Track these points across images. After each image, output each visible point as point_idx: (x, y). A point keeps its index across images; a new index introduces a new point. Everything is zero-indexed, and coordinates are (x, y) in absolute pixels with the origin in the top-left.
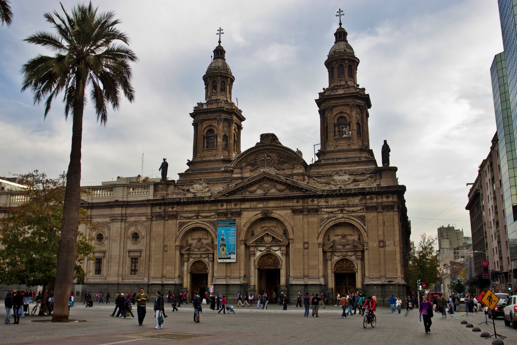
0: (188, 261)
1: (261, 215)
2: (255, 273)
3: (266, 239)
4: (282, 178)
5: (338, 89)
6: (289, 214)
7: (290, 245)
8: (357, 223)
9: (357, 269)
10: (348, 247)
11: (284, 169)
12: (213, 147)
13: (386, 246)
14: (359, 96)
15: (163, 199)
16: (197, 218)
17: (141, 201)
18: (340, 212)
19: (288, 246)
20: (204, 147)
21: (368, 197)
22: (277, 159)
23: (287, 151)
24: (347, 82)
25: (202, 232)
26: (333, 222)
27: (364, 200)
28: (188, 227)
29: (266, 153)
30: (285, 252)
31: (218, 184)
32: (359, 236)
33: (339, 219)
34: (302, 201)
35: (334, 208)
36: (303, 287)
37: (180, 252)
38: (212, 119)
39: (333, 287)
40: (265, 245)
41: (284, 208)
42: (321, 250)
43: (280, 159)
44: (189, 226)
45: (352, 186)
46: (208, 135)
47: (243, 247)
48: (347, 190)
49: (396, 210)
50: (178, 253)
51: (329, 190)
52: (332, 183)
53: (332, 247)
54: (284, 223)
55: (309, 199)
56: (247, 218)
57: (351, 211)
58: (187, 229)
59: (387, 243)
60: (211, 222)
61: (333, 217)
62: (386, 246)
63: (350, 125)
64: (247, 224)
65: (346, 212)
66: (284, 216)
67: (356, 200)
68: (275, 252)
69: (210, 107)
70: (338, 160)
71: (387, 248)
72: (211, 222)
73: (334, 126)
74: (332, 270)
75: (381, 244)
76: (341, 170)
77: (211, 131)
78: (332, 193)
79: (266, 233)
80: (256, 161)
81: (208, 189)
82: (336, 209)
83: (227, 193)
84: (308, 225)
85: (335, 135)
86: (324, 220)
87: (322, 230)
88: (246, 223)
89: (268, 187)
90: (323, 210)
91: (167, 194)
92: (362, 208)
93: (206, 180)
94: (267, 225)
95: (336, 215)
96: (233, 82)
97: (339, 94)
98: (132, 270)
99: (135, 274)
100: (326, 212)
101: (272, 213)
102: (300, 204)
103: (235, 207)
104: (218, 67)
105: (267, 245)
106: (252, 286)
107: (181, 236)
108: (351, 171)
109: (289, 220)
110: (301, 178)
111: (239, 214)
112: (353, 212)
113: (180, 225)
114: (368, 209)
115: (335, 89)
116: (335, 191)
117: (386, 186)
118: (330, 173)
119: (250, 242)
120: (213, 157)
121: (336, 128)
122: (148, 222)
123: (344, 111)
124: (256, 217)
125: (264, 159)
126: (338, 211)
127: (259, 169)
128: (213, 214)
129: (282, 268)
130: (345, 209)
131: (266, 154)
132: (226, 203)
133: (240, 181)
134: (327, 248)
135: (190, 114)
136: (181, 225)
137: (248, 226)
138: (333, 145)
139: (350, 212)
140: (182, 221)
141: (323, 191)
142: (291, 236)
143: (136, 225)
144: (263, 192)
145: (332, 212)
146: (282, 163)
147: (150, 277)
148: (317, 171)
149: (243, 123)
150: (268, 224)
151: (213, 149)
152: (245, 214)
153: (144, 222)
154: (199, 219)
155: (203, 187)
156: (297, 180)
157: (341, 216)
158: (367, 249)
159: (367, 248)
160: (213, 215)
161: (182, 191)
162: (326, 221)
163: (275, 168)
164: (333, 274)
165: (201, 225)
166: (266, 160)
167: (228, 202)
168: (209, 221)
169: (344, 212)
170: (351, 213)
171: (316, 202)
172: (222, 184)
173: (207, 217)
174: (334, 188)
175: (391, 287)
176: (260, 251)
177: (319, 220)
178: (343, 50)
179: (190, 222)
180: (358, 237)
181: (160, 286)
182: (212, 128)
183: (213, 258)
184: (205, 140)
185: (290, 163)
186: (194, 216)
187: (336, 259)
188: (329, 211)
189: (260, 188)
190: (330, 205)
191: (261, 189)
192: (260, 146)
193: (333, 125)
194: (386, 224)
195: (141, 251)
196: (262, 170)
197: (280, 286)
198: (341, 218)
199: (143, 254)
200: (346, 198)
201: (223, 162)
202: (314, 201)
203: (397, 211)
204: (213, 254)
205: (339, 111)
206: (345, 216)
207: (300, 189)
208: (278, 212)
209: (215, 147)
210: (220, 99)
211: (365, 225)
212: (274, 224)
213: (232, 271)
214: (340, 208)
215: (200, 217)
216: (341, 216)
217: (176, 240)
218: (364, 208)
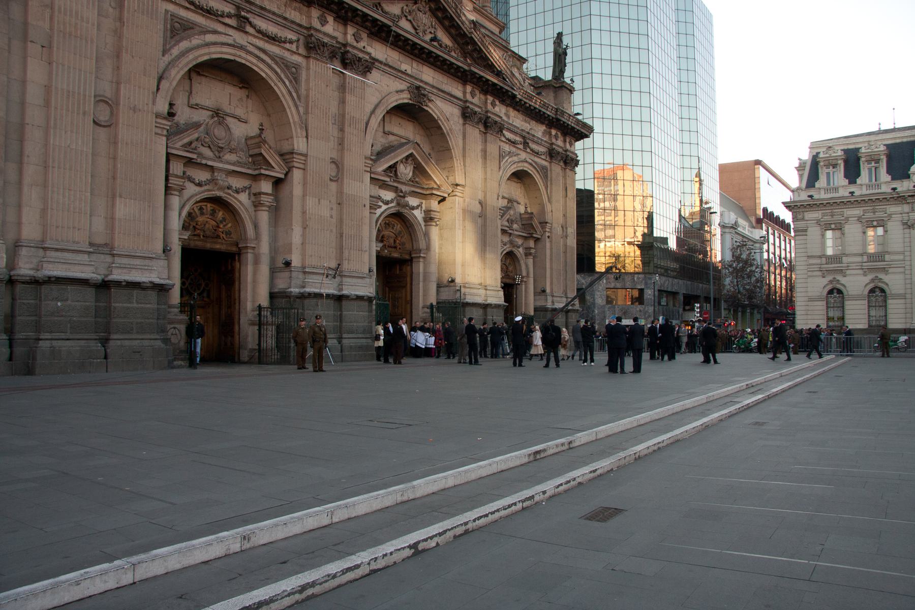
1: (409, 96)
3: (401, 168)
4: (464, 18)
6: (456, 119)
16: (240, 29)
18: (521, 147)
21: (554, 132)
28: (205, 50)
40: (400, 186)
41: (450, 97)
44: (213, 49)
54: (449, 139)
56: (378, 91)
58: (204, 55)
60: (287, 66)
61: (515, 156)
67: (539, 130)
78: (527, 101)
79: (410, 152)
95: (519, 152)
100: (508, 139)
101: (430, 101)
102: (476, 100)
103: (355, 44)
113: (172, 27)
124: (396, 97)
128: (291, 36)
132: (332, 18)
140: (183, 13)
154: (246, 33)
160: (291, 42)
162: (507, 160)
165: (254, 61)
168: (282, 58)
171: (497, 109)
173: (273, 39)
176: (387, 203)
179: (215, 32)
181: (90, 292)
186: (229, 16)
189: (409, 18)
190: (512, 125)
191: (410, 21)
206: (528, 160)
207: (490, 67)
208: (439, 103)
214: (524, 137)
215: (249, 29)
216: (523, 155)
217: (158, 89)
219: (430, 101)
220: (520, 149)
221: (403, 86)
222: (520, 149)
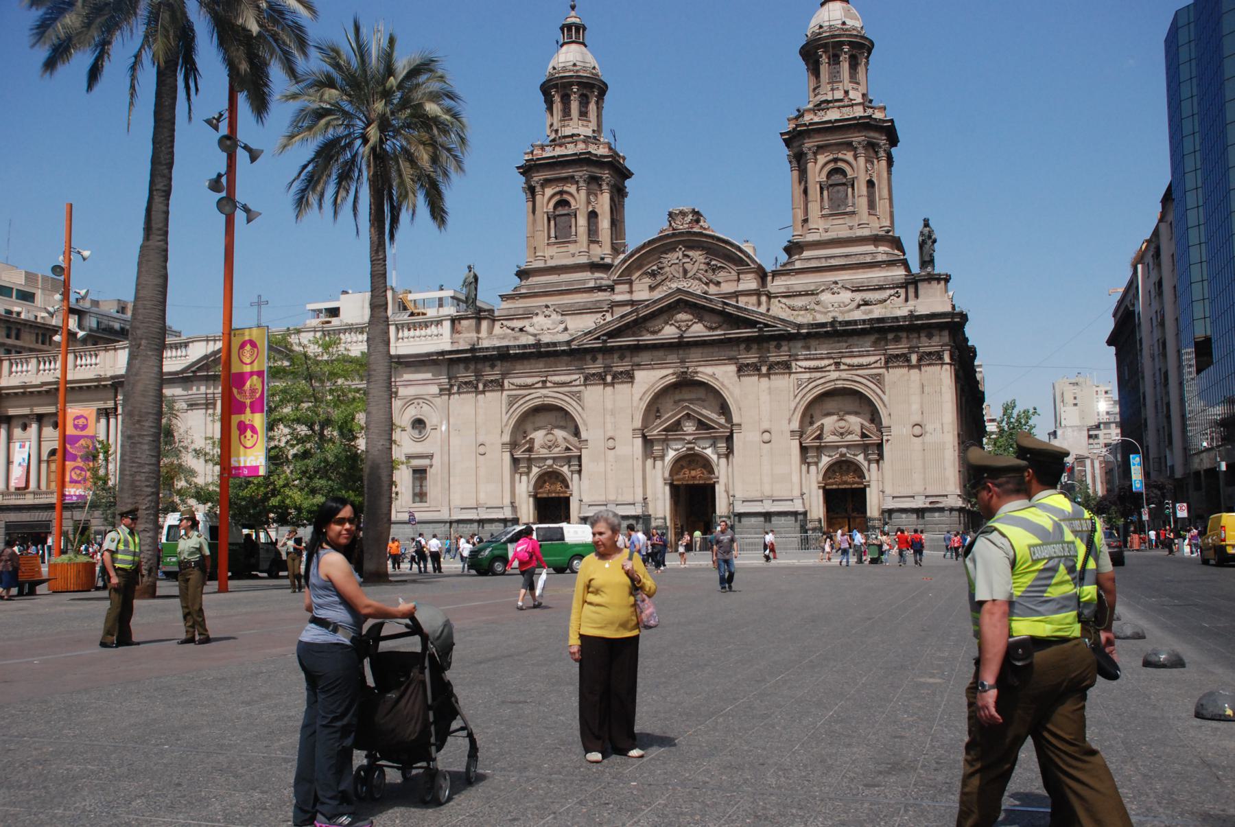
0: (528, 474)
2: (664, 493)
5: (828, 109)
7: (735, 435)
8: (869, 389)
9: (869, 482)
10: (849, 437)
11: (718, 284)
12: (570, 237)
13: (926, 432)
14: (873, 123)
15: (473, 350)
16: (544, 387)
17: (426, 353)
18: (833, 367)
19: (729, 439)
20: (549, 237)
21: (890, 336)
22: (703, 261)
23: (723, 245)
24: (846, 92)
25: (554, 414)
26: (820, 387)
27: (883, 343)
29: (680, 249)
30: (723, 451)
31: (584, 316)
32: (872, 415)
33: (834, 381)
34: (756, 347)
35: (822, 359)
36: (762, 519)
37: (512, 455)
38: (565, 180)
39: (822, 516)
42: (796, 444)
43: (711, 260)
45: (858, 315)
46: (557, 213)
47: (639, 442)
48: (848, 323)
49: (947, 359)
50: (507, 456)
51: (812, 324)
52: (817, 308)
53: (819, 437)
55: (771, 343)
57: (857, 366)
58: (525, 408)
59: (929, 428)
60: (573, 394)
62: (926, 432)
63: (853, 186)
64: (647, 396)
65: (846, 367)
66: (721, 379)
68: (704, 451)
69: (559, 153)
70: (829, 261)
71: (928, 438)
72: (572, 395)
73: (822, 189)
74: (819, 483)
75: (917, 430)
76: (836, 283)
77: (563, 203)
80: (660, 265)
81: (563, 326)
82: (826, 362)
83: (603, 335)
84: (770, 393)
85: (822, 208)
86: (801, 385)
87: (799, 403)
88: (644, 394)
89: (686, 321)
90: (799, 363)
91: (479, 338)
92: (878, 358)
93: (559, 308)
94: (687, 397)
95: (827, 374)
96: (604, 94)
97: (829, 122)
98: (415, 495)
99: (421, 502)
100: (805, 368)
104: (572, 63)
105: (687, 438)
106: (661, 518)
107: (512, 422)
108: (856, 283)
109: (730, 386)
110: (754, 299)
111: (629, 377)
112: (861, 366)
114: (890, 361)
115: (823, 110)
116: (823, 325)
117: (927, 315)
118: (812, 288)
119: (654, 433)
120: (568, 257)
121: (825, 193)
122: (443, 397)
123: (840, 156)
125: (677, 261)
126: (829, 365)
127: (669, 283)
129: (718, 482)
130: (844, 360)
131: (681, 253)
133: (628, 309)
134: (808, 441)
135: (518, 168)
136: (512, 401)
137: (648, 398)
138: (818, 229)
139: (853, 366)
141: (800, 326)
142: (735, 420)
143: (418, 404)
144: (677, 331)
145: (817, 369)
146: (714, 270)
147: (452, 507)
148: (785, 283)
149: (627, 183)
150: (687, 394)
151: (569, 242)
152: (640, 375)
153: (434, 396)
155: (554, 323)
156: (747, 303)
157: (834, 375)
158: (887, 441)
159: (889, 437)
161: (510, 331)
163: (700, 280)
164: (821, 491)
166: (681, 264)
167: (607, 351)
169: (842, 367)
170: (857, 370)
172: (593, 315)
174: (821, 319)
175: (937, 514)
177: (791, 385)
178: (840, 22)
179: (530, 394)
180: (870, 416)
181: (476, 525)
182: (566, 197)
183: (580, 466)
184: (552, 223)
185: (731, 270)
186: (537, 383)
187: (825, 460)
188: (812, 366)
191: (672, 324)
192: (667, 236)
193: (818, 186)
194: (926, 389)
195: (431, 457)
196: (674, 286)
197: (715, 517)
198: (837, 380)
199: (436, 461)
200: (845, 338)
201: (591, 268)
202: (781, 346)
203: (948, 364)
204: (580, 458)
205: (831, 157)
206: (844, 375)
207: (752, 324)
208: (709, 370)
209: (573, 238)
210: (579, 135)
211: (884, 392)
212: (701, 393)
213: (620, 491)
214: (834, 358)
216: (834, 375)
218: (883, 358)
219: (697, 373)
220: (829, 371)
221: (671, 371)
222: (829, 371)
